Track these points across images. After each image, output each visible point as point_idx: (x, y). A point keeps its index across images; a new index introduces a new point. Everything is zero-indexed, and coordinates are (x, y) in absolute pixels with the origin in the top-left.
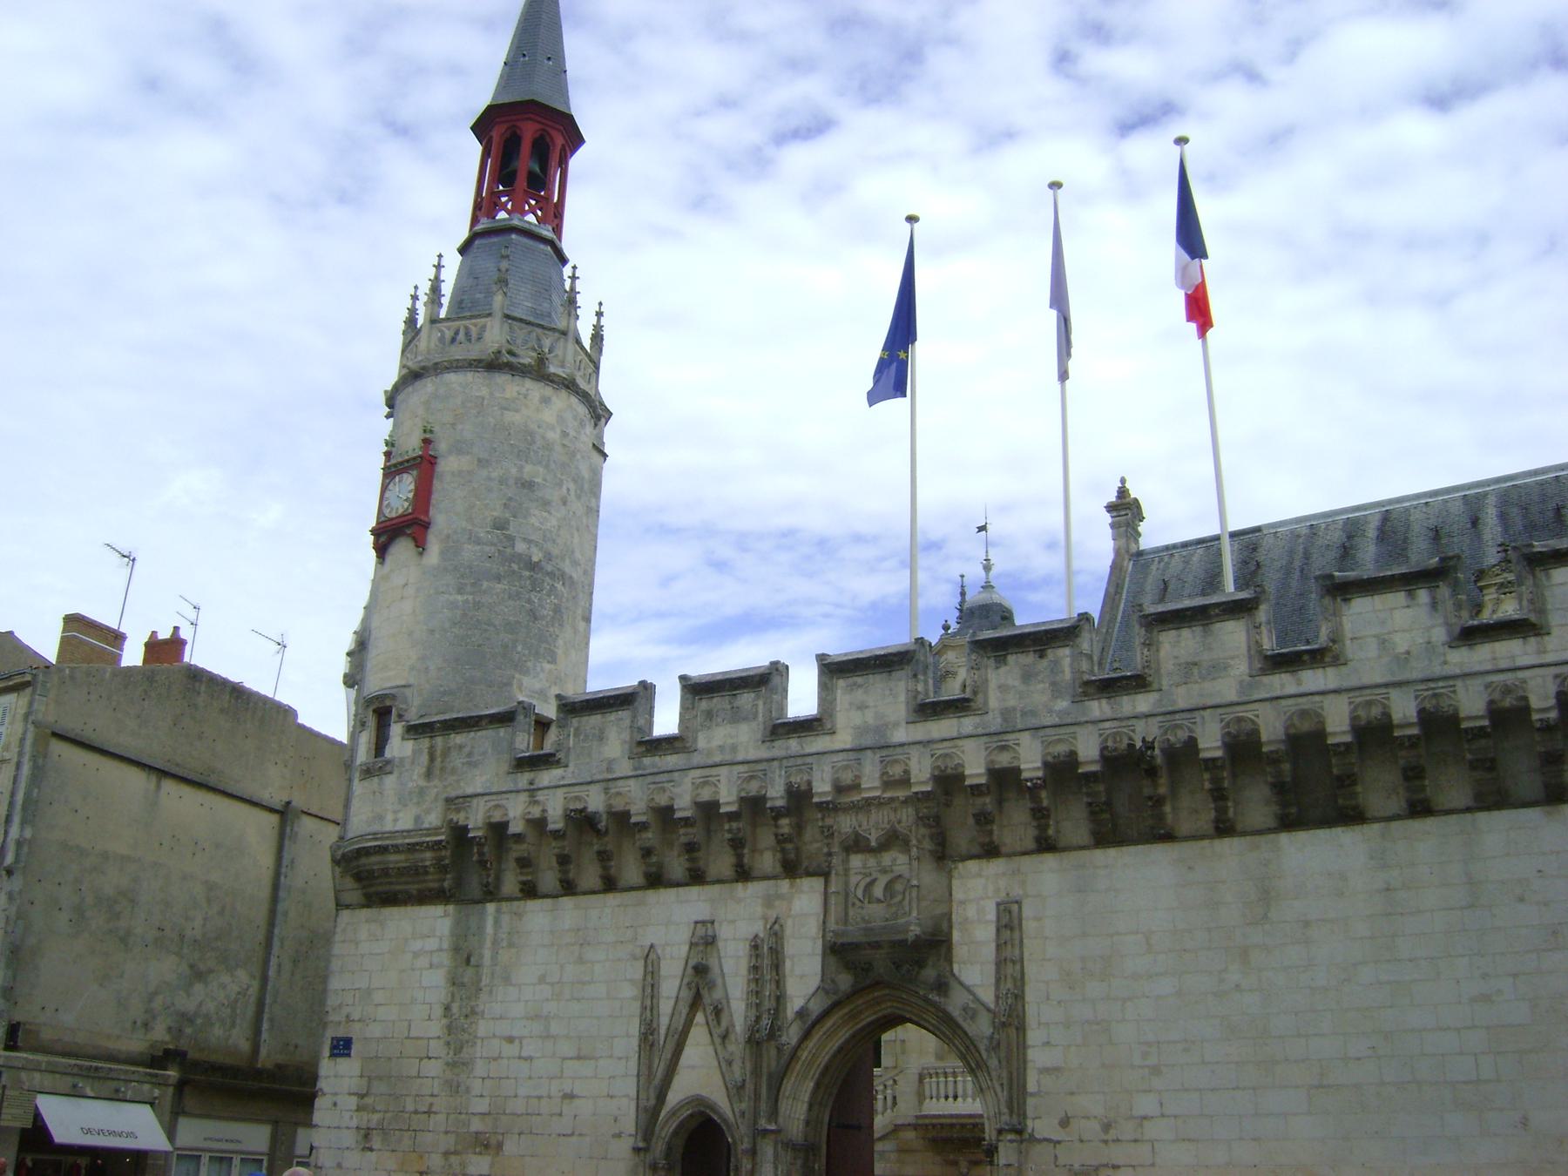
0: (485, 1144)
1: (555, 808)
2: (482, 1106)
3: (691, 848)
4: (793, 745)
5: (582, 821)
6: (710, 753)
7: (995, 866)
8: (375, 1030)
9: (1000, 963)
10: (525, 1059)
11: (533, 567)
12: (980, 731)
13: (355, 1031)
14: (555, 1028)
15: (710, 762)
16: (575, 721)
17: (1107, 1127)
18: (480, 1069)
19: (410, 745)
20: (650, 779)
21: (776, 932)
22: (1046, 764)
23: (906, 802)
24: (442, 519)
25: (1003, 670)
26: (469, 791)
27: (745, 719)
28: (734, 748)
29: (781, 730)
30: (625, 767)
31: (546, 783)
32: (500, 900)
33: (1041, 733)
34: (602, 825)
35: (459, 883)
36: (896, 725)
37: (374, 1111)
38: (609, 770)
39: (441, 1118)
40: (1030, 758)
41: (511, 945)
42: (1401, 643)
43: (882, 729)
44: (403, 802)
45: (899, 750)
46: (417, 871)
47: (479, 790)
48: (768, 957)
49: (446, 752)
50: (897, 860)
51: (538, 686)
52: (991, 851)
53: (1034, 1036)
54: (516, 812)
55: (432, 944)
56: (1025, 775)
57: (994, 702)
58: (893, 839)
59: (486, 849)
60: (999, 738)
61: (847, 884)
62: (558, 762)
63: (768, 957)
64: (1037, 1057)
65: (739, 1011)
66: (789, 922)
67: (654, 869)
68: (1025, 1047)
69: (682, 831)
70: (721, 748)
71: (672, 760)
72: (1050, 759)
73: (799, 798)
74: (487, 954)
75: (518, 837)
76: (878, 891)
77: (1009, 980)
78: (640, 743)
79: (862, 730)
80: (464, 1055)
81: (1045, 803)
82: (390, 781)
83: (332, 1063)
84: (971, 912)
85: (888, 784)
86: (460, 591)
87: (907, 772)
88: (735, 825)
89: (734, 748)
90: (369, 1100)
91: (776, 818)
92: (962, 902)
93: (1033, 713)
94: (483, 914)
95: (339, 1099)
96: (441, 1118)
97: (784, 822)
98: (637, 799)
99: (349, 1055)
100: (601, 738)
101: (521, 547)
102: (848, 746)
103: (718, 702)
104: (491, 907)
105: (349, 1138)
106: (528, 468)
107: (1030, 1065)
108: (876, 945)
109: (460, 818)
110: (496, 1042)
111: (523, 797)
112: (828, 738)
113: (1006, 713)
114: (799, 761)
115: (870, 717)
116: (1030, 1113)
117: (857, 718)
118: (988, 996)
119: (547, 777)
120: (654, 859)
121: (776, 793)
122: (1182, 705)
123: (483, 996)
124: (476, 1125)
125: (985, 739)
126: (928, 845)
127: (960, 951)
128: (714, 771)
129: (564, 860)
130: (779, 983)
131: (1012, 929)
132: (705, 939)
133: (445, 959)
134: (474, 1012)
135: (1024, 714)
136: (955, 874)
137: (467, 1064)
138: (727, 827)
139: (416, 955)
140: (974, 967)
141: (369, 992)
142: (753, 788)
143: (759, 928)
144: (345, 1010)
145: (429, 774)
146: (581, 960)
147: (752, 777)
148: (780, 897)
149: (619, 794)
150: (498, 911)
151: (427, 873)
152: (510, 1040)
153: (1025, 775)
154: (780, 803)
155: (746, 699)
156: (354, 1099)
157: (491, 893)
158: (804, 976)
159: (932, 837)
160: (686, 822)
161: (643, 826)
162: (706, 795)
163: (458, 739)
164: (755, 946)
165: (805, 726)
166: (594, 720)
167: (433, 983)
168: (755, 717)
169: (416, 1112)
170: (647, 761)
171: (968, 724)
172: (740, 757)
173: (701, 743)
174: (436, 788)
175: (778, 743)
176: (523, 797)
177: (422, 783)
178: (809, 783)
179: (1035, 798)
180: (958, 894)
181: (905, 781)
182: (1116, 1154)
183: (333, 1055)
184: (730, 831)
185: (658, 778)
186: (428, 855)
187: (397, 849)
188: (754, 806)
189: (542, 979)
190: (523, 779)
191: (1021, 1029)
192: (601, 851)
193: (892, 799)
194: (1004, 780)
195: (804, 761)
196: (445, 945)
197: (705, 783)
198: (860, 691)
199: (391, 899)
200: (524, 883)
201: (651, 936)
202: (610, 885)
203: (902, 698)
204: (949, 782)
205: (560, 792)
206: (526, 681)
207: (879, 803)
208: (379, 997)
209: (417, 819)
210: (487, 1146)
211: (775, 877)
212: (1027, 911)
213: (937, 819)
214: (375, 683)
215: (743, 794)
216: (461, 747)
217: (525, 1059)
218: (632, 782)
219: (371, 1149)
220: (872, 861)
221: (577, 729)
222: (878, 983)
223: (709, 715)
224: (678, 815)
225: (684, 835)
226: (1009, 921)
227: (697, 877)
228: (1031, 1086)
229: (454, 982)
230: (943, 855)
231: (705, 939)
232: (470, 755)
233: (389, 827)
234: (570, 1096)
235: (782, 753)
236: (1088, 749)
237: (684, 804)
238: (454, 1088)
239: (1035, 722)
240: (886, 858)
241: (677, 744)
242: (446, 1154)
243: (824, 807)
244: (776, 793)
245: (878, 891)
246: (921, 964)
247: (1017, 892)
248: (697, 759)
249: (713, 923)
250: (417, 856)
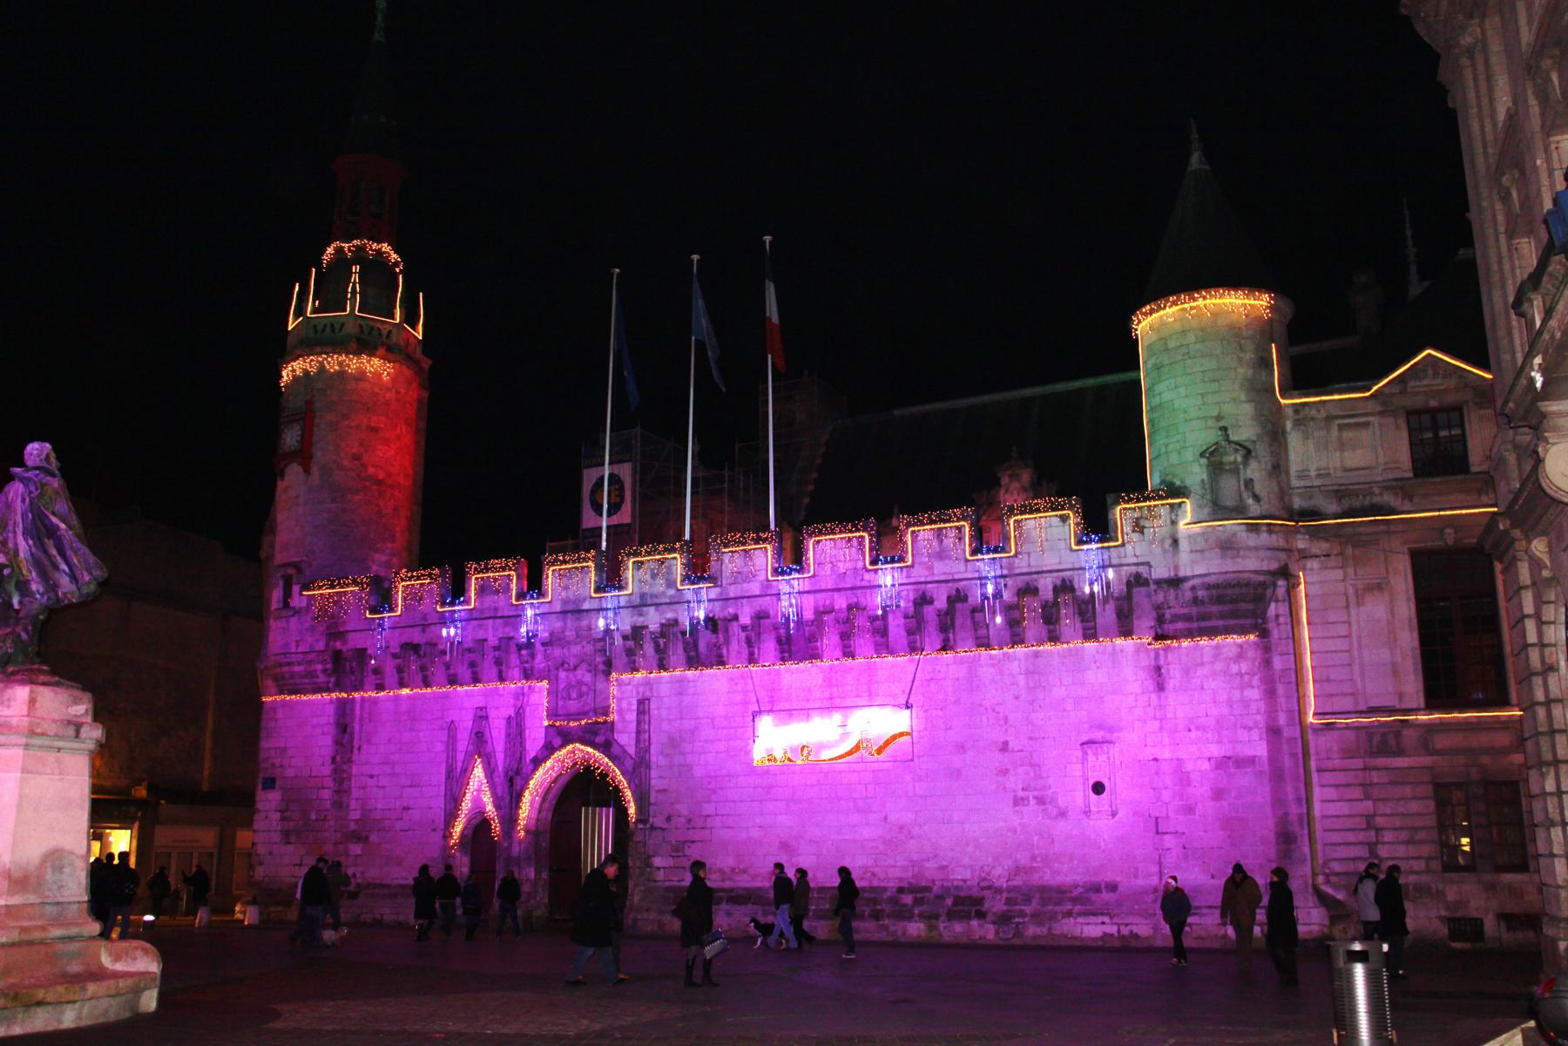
0: (358, 837)
2: (357, 815)
8: (290, 773)
11: (379, 482)
14: (398, 769)
17: (689, 821)
18: (355, 793)
24: (320, 456)
38: (425, 618)
42: (842, 568)
51: (384, 558)
55: (324, 720)
74: (357, 726)
79: (565, 602)
82: (293, 621)
101: (371, 470)
105: (276, 837)
106: (374, 418)
118: (632, 751)
122: (732, 595)
124: (353, 826)
130: (522, 744)
132: (482, 716)
133: (331, 730)
137: (347, 792)
141: (284, 750)
143: (512, 712)
146: (412, 730)
152: (371, 776)
182: (693, 835)
189: (389, 741)
206: (377, 557)
229: (338, 743)
231: (482, 716)
234: (406, 809)
238: (339, 804)
242: (336, 844)
247: (648, 694)
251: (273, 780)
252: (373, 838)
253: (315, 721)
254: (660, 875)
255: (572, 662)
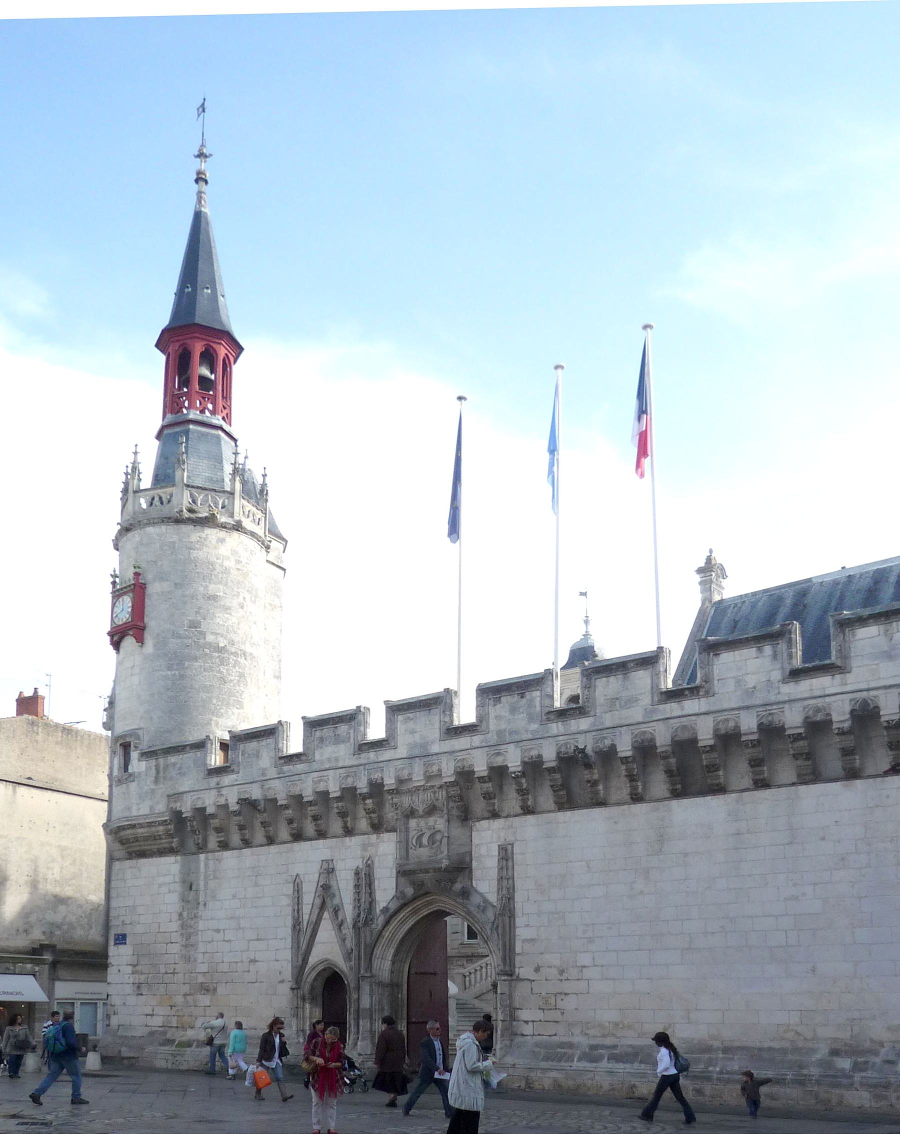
1: (232, 798)
2: (204, 968)
3: (315, 818)
4: (372, 755)
5: (249, 804)
6: (322, 762)
7: (498, 823)
8: (139, 929)
9: (500, 879)
10: (227, 941)
12: (484, 744)
13: (127, 930)
14: (243, 923)
15: (323, 768)
16: (242, 746)
17: (562, 972)
18: (201, 947)
19: (143, 764)
20: (287, 779)
21: (369, 866)
22: (524, 763)
23: (441, 787)
25: (498, 706)
26: (182, 789)
27: (343, 741)
28: (337, 759)
29: (364, 748)
30: (272, 773)
31: (226, 783)
32: (208, 852)
33: (521, 744)
34: (261, 806)
35: (182, 844)
36: (433, 742)
37: (142, 974)
39: (181, 975)
40: (513, 760)
41: (215, 878)
43: (424, 745)
44: (142, 797)
45: (435, 757)
46: (155, 838)
47: (188, 790)
48: (365, 879)
49: (166, 767)
50: (439, 822)
52: (495, 815)
53: (519, 921)
54: (209, 801)
55: (169, 879)
56: (511, 770)
57: (492, 727)
58: (432, 810)
59: (195, 823)
60: (496, 748)
61: (407, 836)
62: (233, 771)
63: (365, 879)
64: (522, 933)
65: (349, 912)
66: (377, 859)
67: (295, 831)
68: (515, 928)
69: (309, 808)
70: (329, 760)
71: (300, 767)
72: (526, 759)
73: (377, 788)
74: (202, 883)
75: (212, 816)
76: (425, 841)
77: (504, 889)
78: (281, 758)
79: (412, 746)
80: (192, 940)
81: (525, 786)
83: (116, 948)
84: (483, 850)
85: (428, 778)
86: (170, 668)
87: (440, 770)
88: (340, 804)
89: (337, 759)
90: (139, 968)
91: (364, 799)
92: (478, 845)
93: (516, 732)
94: (198, 861)
95: (121, 968)
96: (181, 975)
97: (369, 801)
98: (280, 791)
99: (125, 943)
100: (257, 755)
102: (405, 756)
103: (327, 731)
104: (202, 857)
105: (129, 989)
107: (517, 938)
108: (427, 871)
109: (178, 806)
110: (210, 933)
111: (214, 792)
112: (392, 751)
113: (500, 733)
114: (376, 766)
115: (417, 738)
116: (517, 965)
117: (409, 739)
118: (493, 898)
119: (227, 779)
120: (295, 825)
121: (362, 786)
123: (201, 907)
124: (201, 979)
125: (487, 749)
126: (455, 812)
127: (477, 873)
128: (325, 773)
129: (242, 828)
131: (507, 860)
133: (178, 887)
134: (195, 917)
135: (511, 733)
136: (474, 829)
138: (335, 805)
139: (160, 885)
140: (485, 882)
141: (134, 907)
142: (349, 782)
143: (359, 863)
144: (121, 918)
145: (156, 781)
146: (256, 885)
147: (348, 776)
148: (371, 845)
149: (270, 788)
150: (207, 859)
151: (161, 839)
152: (218, 931)
153: (511, 770)
154: (365, 790)
155: (343, 728)
156: (130, 968)
157: (202, 848)
158: (386, 891)
159: (457, 807)
160: (310, 803)
161: (286, 807)
162: (321, 787)
163: (172, 759)
164: (357, 873)
165: (378, 744)
166: (253, 745)
167: (171, 901)
168: (349, 741)
169: (166, 973)
170: (286, 768)
171: (477, 740)
172: (340, 765)
173: (317, 757)
174: (163, 789)
175: (363, 755)
176: (214, 792)
177: (153, 786)
178: (382, 779)
179: (519, 784)
180: (475, 840)
181: (439, 775)
183: (115, 944)
184: (337, 808)
185: (292, 778)
186: (161, 828)
187: (141, 826)
188: (349, 793)
189: (234, 896)
190: (214, 781)
191: (512, 916)
192: (262, 821)
193: (433, 787)
194: (499, 773)
195: (379, 765)
196: (177, 879)
197: (321, 780)
198: (411, 722)
199: (142, 854)
200: (220, 842)
201: (298, 869)
202: (271, 841)
203: (437, 726)
204: (465, 776)
205: (235, 787)
207: (425, 789)
208: (140, 910)
209: (151, 808)
210: (208, 990)
211: (367, 834)
212: (517, 850)
213: (461, 798)
214: (121, 728)
215: (343, 786)
216: (174, 764)
217: (227, 941)
218: (277, 781)
219: (142, 995)
220: (422, 823)
221: (243, 751)
222: (427, 893)
223: (322, 740)
224: (305, 800)
225: (312, 810)
226: (506, 855)
227: (321, 834)
228: (518, 949)
229: (184, 900)
230: (466, 816)
232: (180, 768)
233: (134, 813)
235: (366, 761)
236: (549, 754)
237: (308, 795)
238: (187, 959)
239: (516, 738)
240: (431, 821)
241: (303, 758)
243: (395, 792)
244: (362, 786)
245: (425, 841)
246: (453, 882)
248: (315, 766)
249: (332, 860)
250: (153, 829)
251: (124, 936)
252: (221, 990)
253: (161, 880)
254: (528, 1029)
255: (421, 809)
